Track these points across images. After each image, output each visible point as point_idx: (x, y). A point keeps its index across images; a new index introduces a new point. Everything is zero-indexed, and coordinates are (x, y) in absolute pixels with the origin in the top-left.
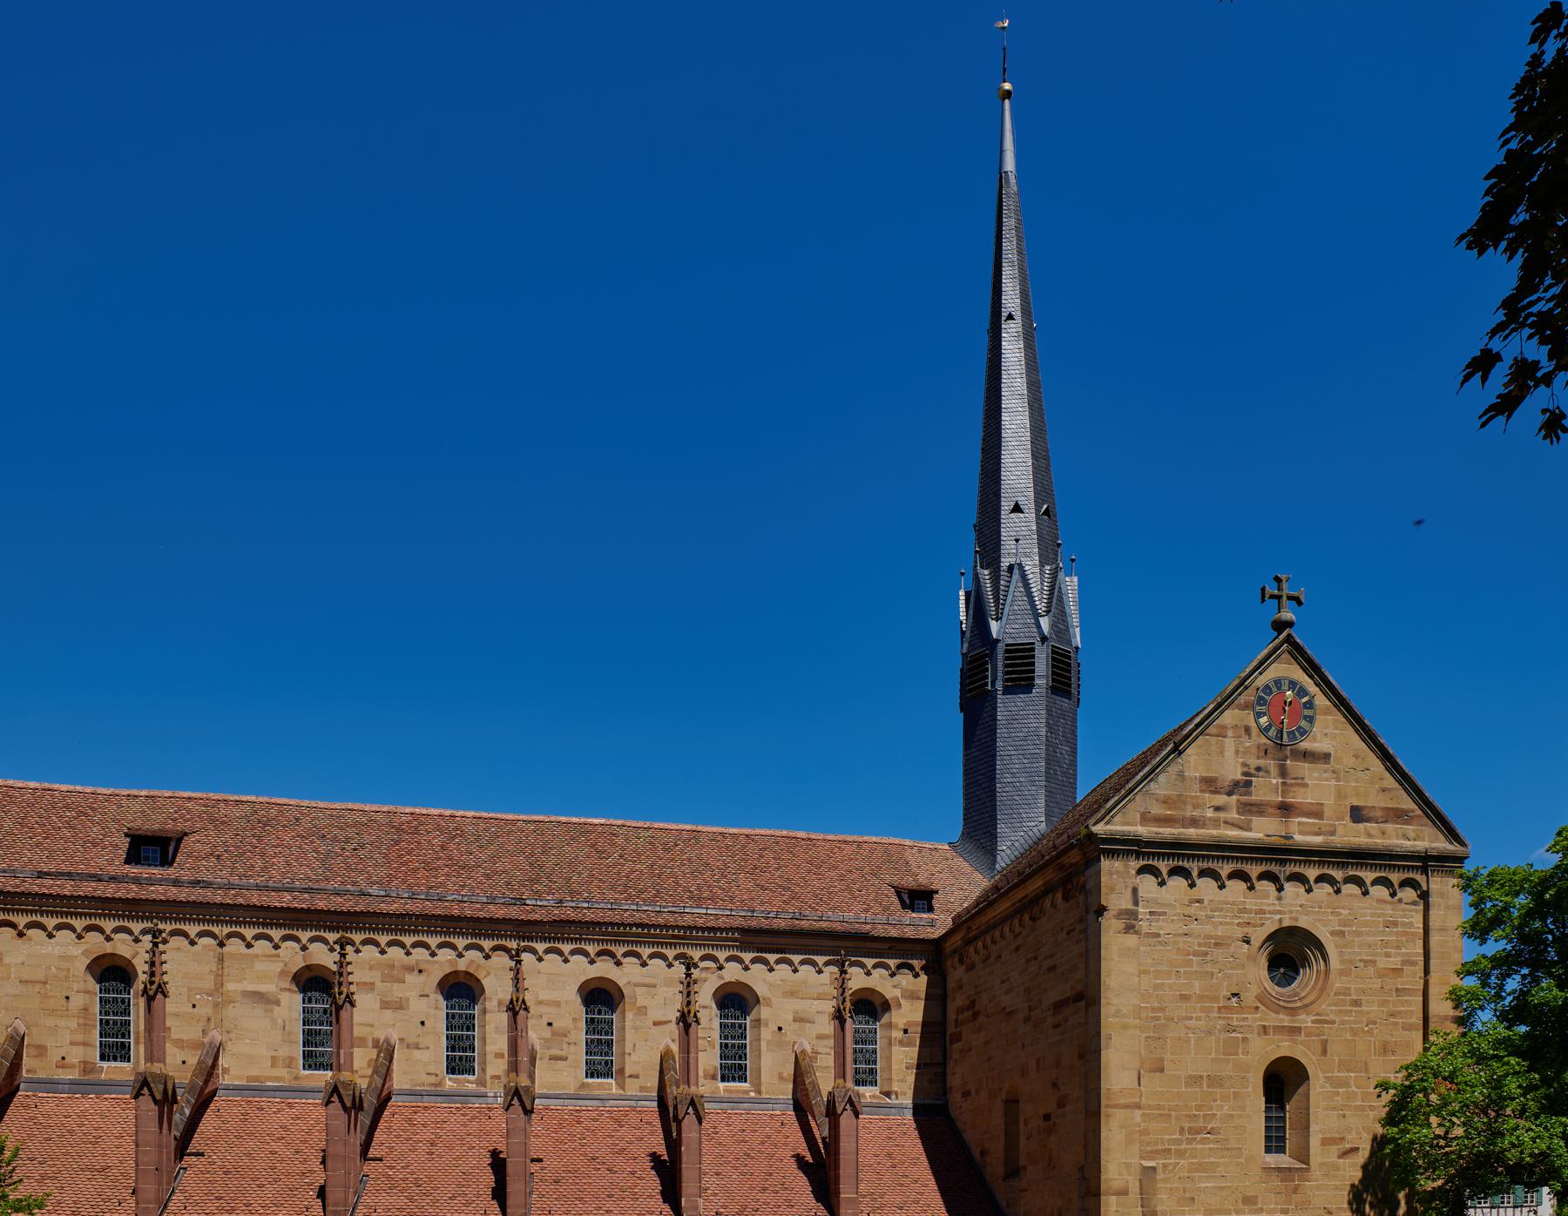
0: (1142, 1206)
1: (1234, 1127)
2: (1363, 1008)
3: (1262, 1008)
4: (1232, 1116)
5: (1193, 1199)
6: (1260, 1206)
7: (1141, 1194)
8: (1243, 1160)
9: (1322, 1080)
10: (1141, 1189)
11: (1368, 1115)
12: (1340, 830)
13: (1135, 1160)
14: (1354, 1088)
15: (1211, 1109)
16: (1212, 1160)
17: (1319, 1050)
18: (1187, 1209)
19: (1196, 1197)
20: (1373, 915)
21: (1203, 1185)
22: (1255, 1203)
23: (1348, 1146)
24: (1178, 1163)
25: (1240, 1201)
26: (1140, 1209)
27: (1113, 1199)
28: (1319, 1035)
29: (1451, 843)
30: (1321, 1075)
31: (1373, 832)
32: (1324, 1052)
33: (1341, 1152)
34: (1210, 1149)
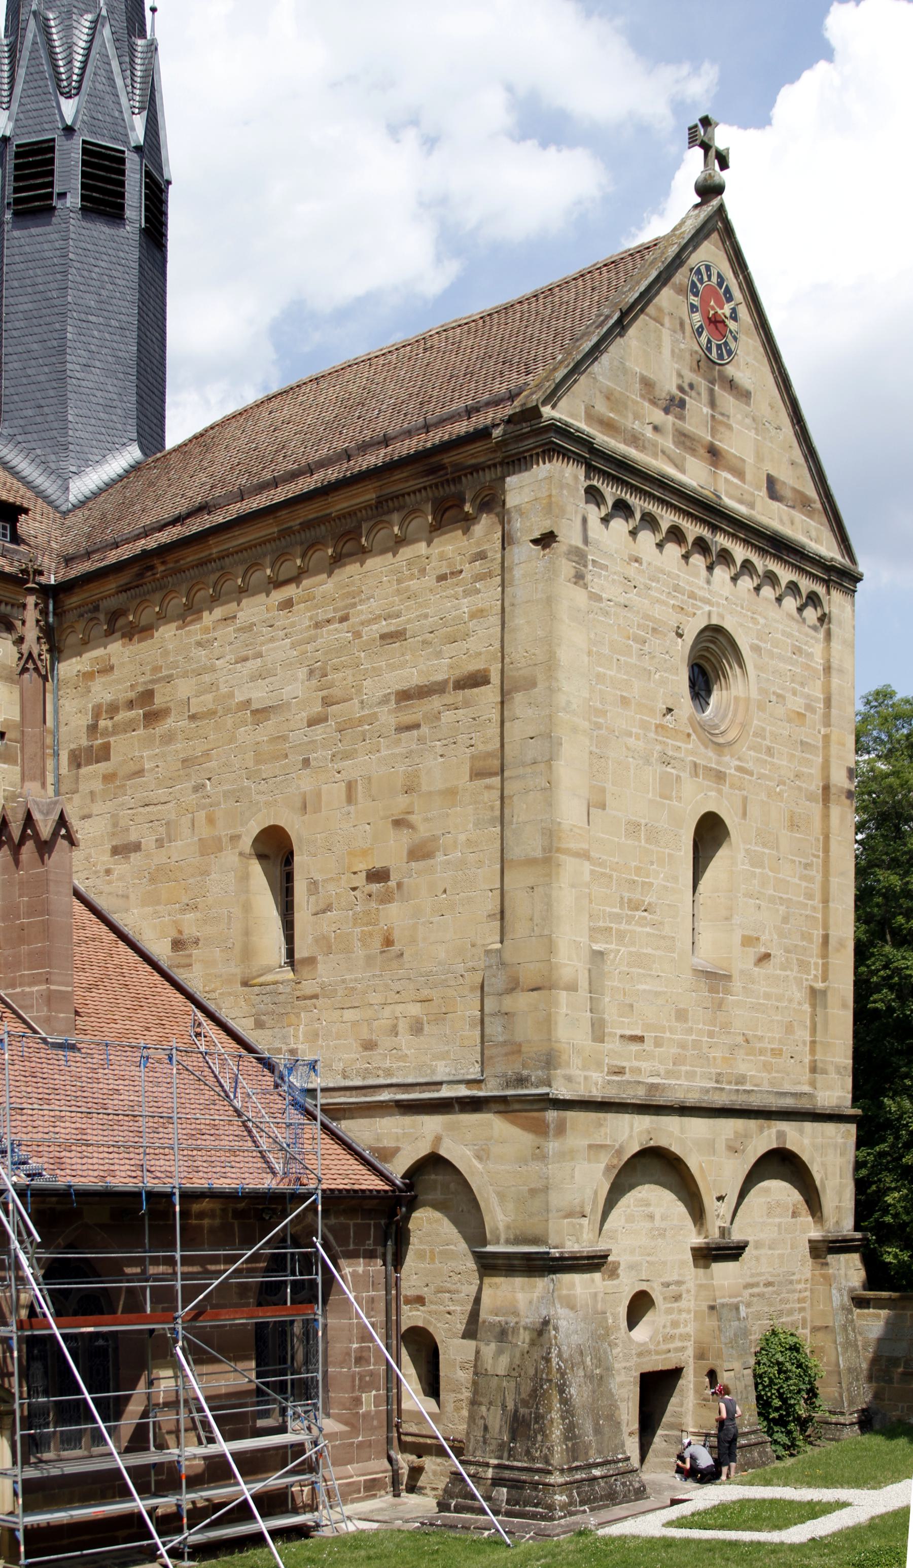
0: (591, 1011)
1: (668, 905)
2: (775, 760)
3: (694, 737)
4: (666, 888)
5: (631, 1006)
6: (690, 1024)
7: (590, 992)
8: (675, 955)
9: (743, 853)
10: (590, 984)
11: (778, 910)
12: (758, 505)
13: (584, 940)
14: (767, 870)
15: (648, 876)
16: (649, 951)
17: (740, 812)
18: (626, 1020)
19: (635, 1004)
20: (784, 633)
21: (642, 987)
22: (686, 1020)
23: (763, 950)
24: (619, 951)
25: (673, 1014)
26: (589, 1014)
27: (563, 996)
28: (740, 789)
29: (843, 557)
30: (742, 846)
31: (785, 518)
32: (744, 814)
33: (758, 956)
34: (648, 934)
